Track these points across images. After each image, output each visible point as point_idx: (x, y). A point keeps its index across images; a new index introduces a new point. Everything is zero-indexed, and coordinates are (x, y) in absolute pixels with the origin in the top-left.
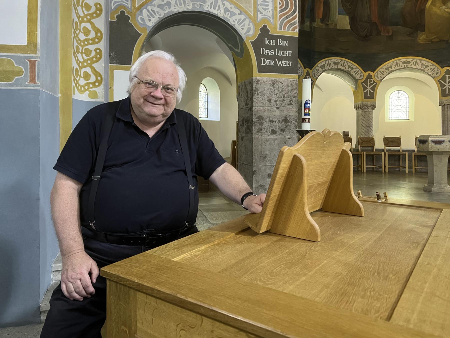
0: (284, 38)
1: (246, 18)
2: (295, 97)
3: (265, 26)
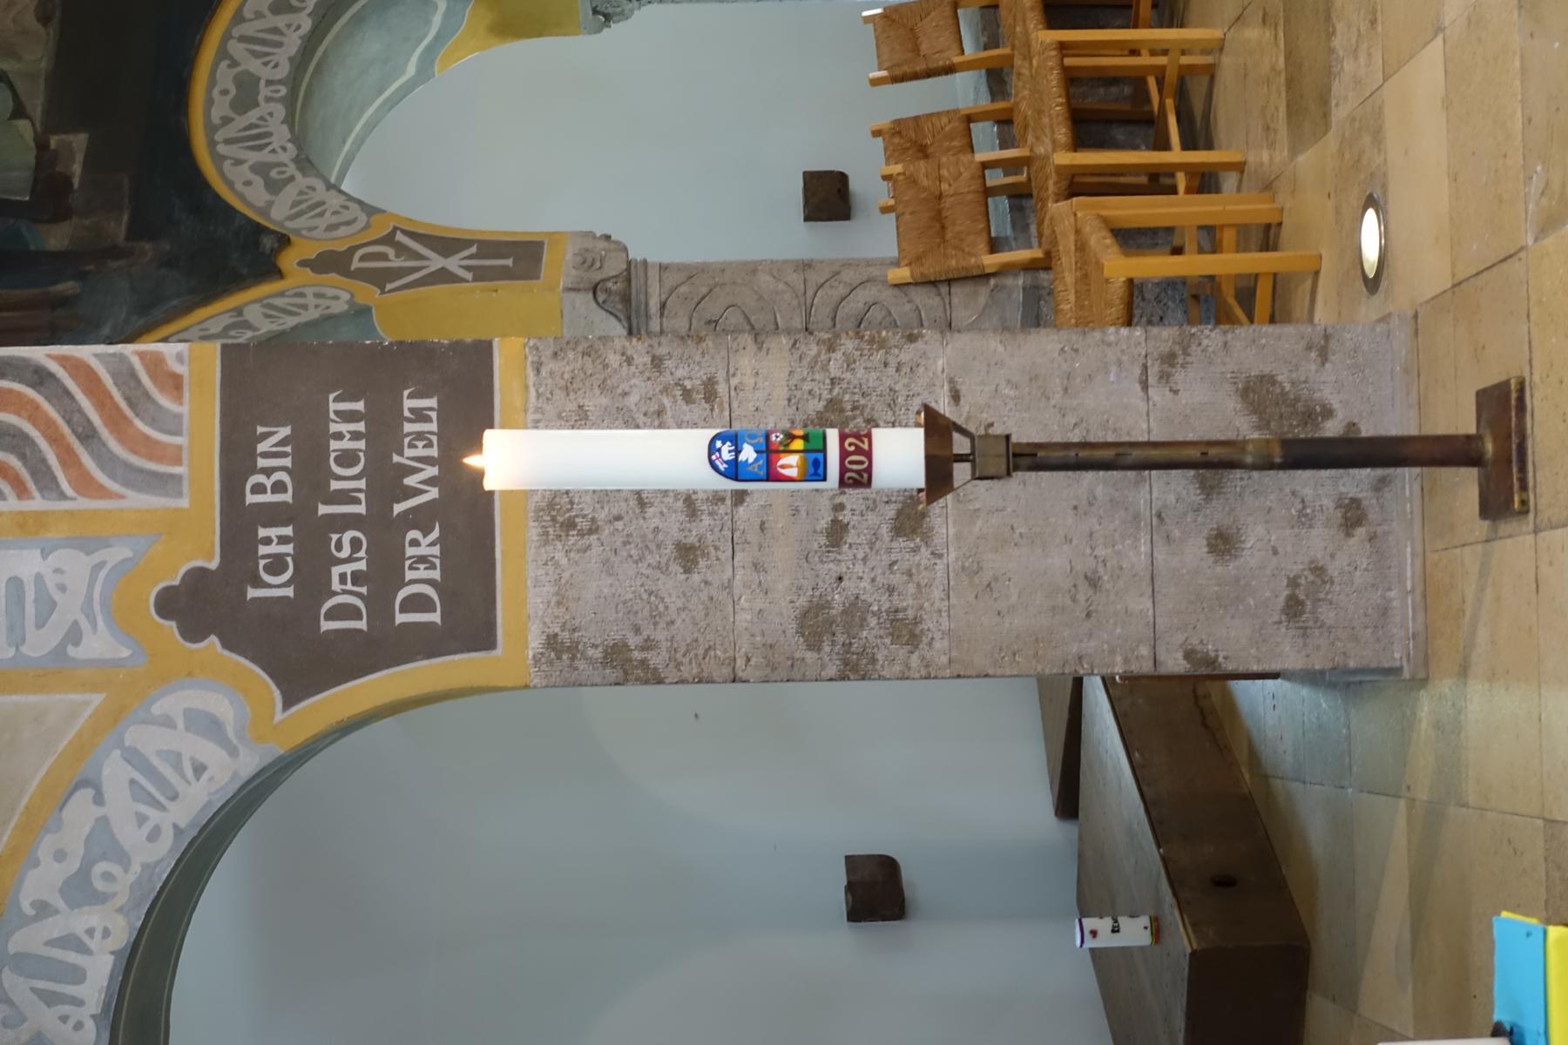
0: (237, 459)
1: (120, 744)
2: (657, 362)
3: (168, 604)
